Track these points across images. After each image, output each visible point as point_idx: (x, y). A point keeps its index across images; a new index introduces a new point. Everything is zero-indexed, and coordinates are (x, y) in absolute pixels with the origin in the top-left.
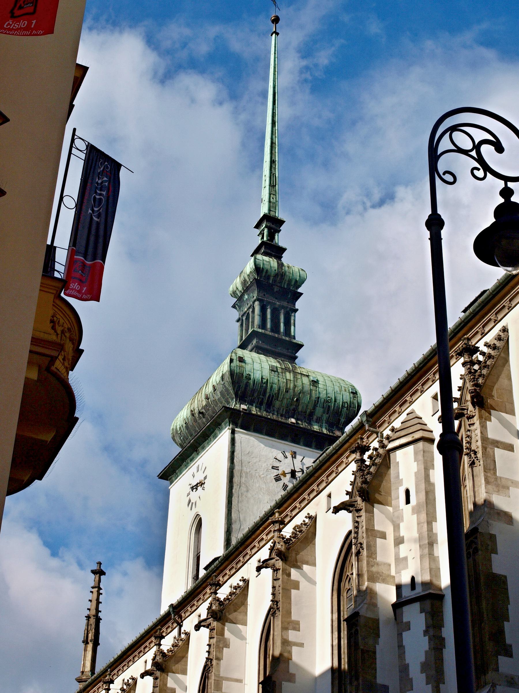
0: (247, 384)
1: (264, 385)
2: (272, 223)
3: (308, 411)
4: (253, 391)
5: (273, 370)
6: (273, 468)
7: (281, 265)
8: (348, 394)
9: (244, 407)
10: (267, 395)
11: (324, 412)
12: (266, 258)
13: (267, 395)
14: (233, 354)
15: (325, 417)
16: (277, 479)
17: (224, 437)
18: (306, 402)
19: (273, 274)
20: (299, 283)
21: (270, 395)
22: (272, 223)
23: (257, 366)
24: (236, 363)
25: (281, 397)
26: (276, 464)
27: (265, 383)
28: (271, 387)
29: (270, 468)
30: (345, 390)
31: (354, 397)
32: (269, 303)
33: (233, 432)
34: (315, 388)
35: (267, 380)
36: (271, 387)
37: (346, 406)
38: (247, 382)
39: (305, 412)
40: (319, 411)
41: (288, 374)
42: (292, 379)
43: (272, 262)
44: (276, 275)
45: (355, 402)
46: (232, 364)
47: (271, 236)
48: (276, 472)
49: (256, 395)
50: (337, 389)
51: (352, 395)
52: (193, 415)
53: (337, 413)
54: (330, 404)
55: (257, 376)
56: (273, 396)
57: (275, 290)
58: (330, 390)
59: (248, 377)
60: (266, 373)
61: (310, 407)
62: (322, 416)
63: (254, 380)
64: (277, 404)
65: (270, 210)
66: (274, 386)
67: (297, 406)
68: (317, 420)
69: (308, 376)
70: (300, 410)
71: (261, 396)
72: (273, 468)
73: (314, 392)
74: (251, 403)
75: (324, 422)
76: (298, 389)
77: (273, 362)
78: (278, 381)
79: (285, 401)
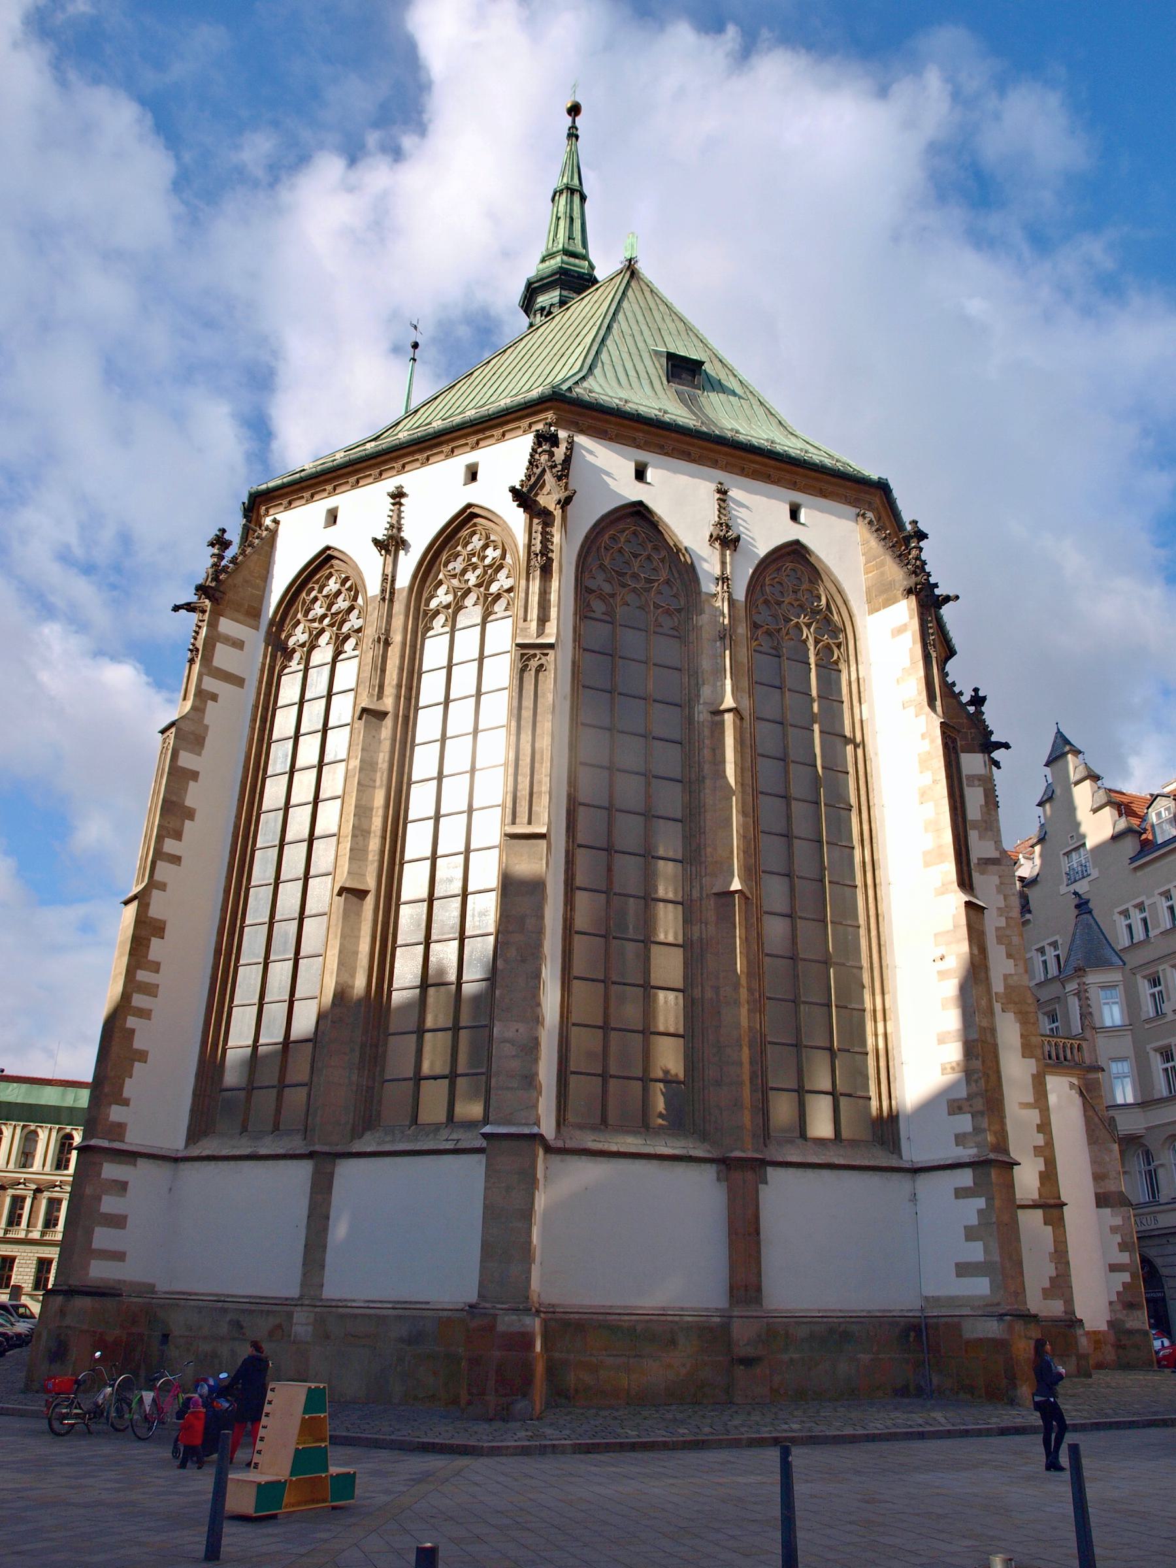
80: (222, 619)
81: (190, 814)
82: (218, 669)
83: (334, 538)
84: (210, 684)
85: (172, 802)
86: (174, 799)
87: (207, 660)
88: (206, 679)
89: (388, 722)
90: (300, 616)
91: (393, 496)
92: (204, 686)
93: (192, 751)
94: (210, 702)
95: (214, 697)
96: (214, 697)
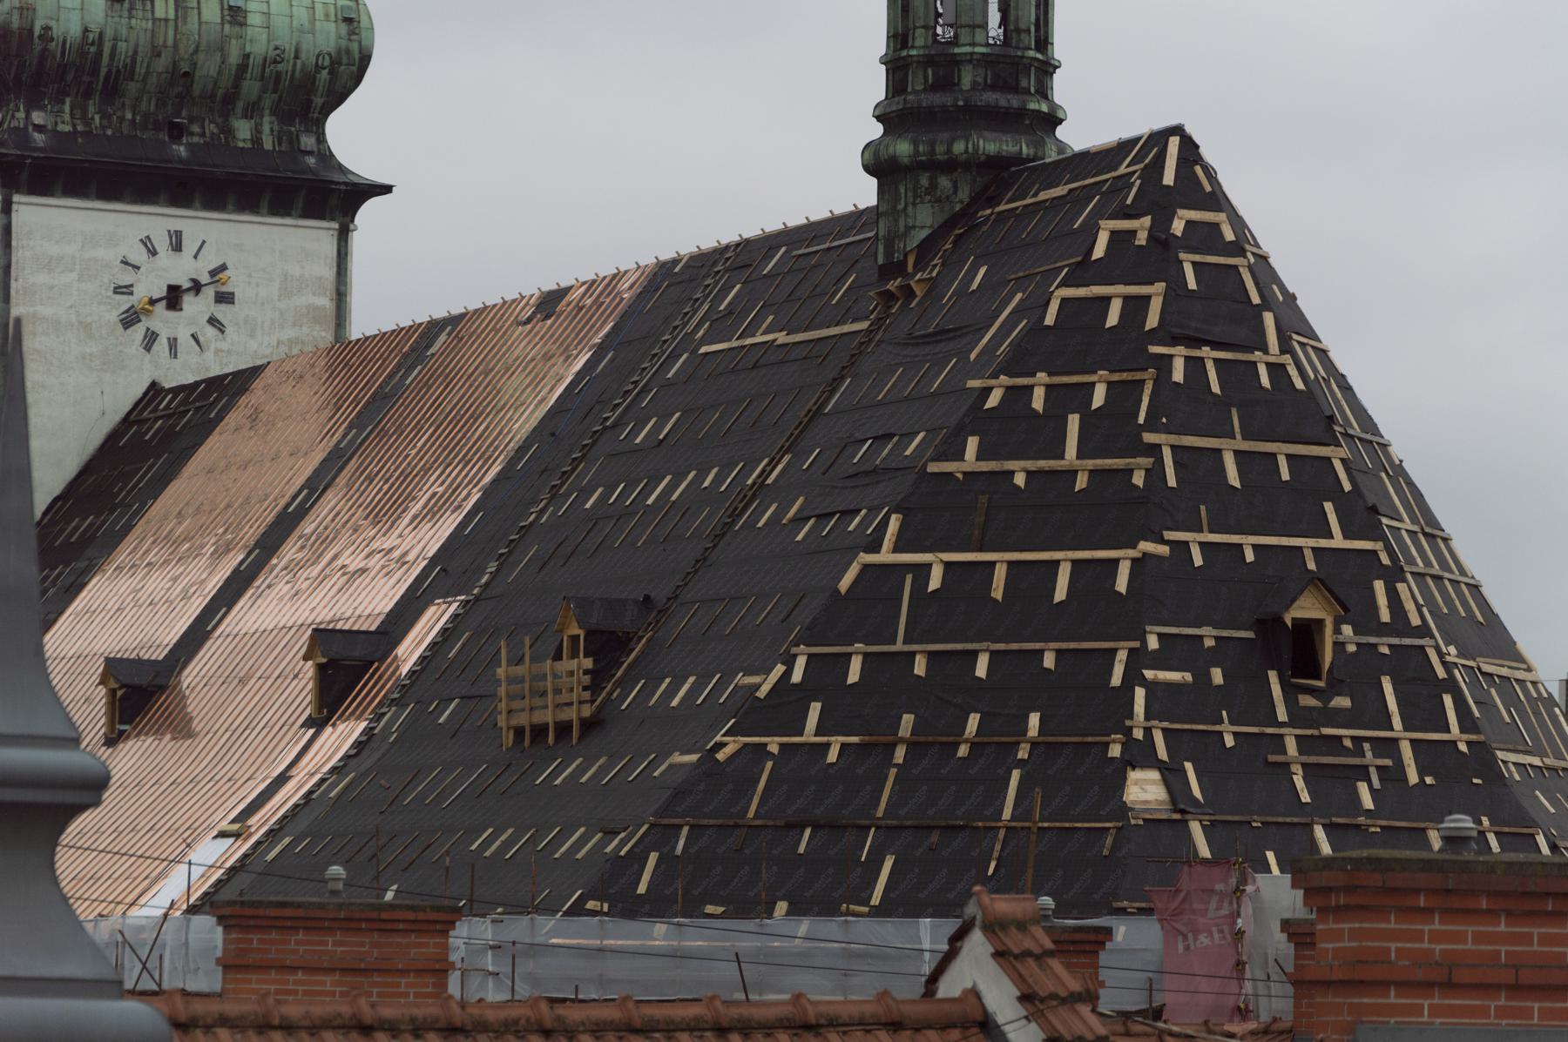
1: (93, 49)
3: (220, 93)
6: (121, 290)
8: (332, 26)
10: (104, 71)
11: (264, 90)
13: (104, 71)
15: (267, 102)
16: (130, 319)
18: (213, 72)
21: (109, 71)
25: (140, 70)
26: (127, 278)
27: (93, 44)
28: (114, 49)
29: (110, 293)
30: (327, 15)
31: (352, 33)
34: (237, 29)
35: (101, 34)
36: (114, 49)
37: (327, 63)
38: (45, 50)
39: (213, 96)
40: (250, 87)
42: (171, 15)
45: (355, 47)
48: (125, 302)
49: (70, 76)
50: (301, 15)
51: (344, 28)
53: (306, 82)
54: (280, 67)
55: (70, 27)
56: (118, 72)
58: (281, 24)
61: (226, 82)
62: (260, 98)
63: (64, 42)
66: (122, 46)
67: (189, 88)
68: (246, 110)
70: (197, 90)
71: (86, 79)
72: (121, 290)
73: (233, 41)
75: (267, 112)
76: (186, 48)
79: (153, 79)
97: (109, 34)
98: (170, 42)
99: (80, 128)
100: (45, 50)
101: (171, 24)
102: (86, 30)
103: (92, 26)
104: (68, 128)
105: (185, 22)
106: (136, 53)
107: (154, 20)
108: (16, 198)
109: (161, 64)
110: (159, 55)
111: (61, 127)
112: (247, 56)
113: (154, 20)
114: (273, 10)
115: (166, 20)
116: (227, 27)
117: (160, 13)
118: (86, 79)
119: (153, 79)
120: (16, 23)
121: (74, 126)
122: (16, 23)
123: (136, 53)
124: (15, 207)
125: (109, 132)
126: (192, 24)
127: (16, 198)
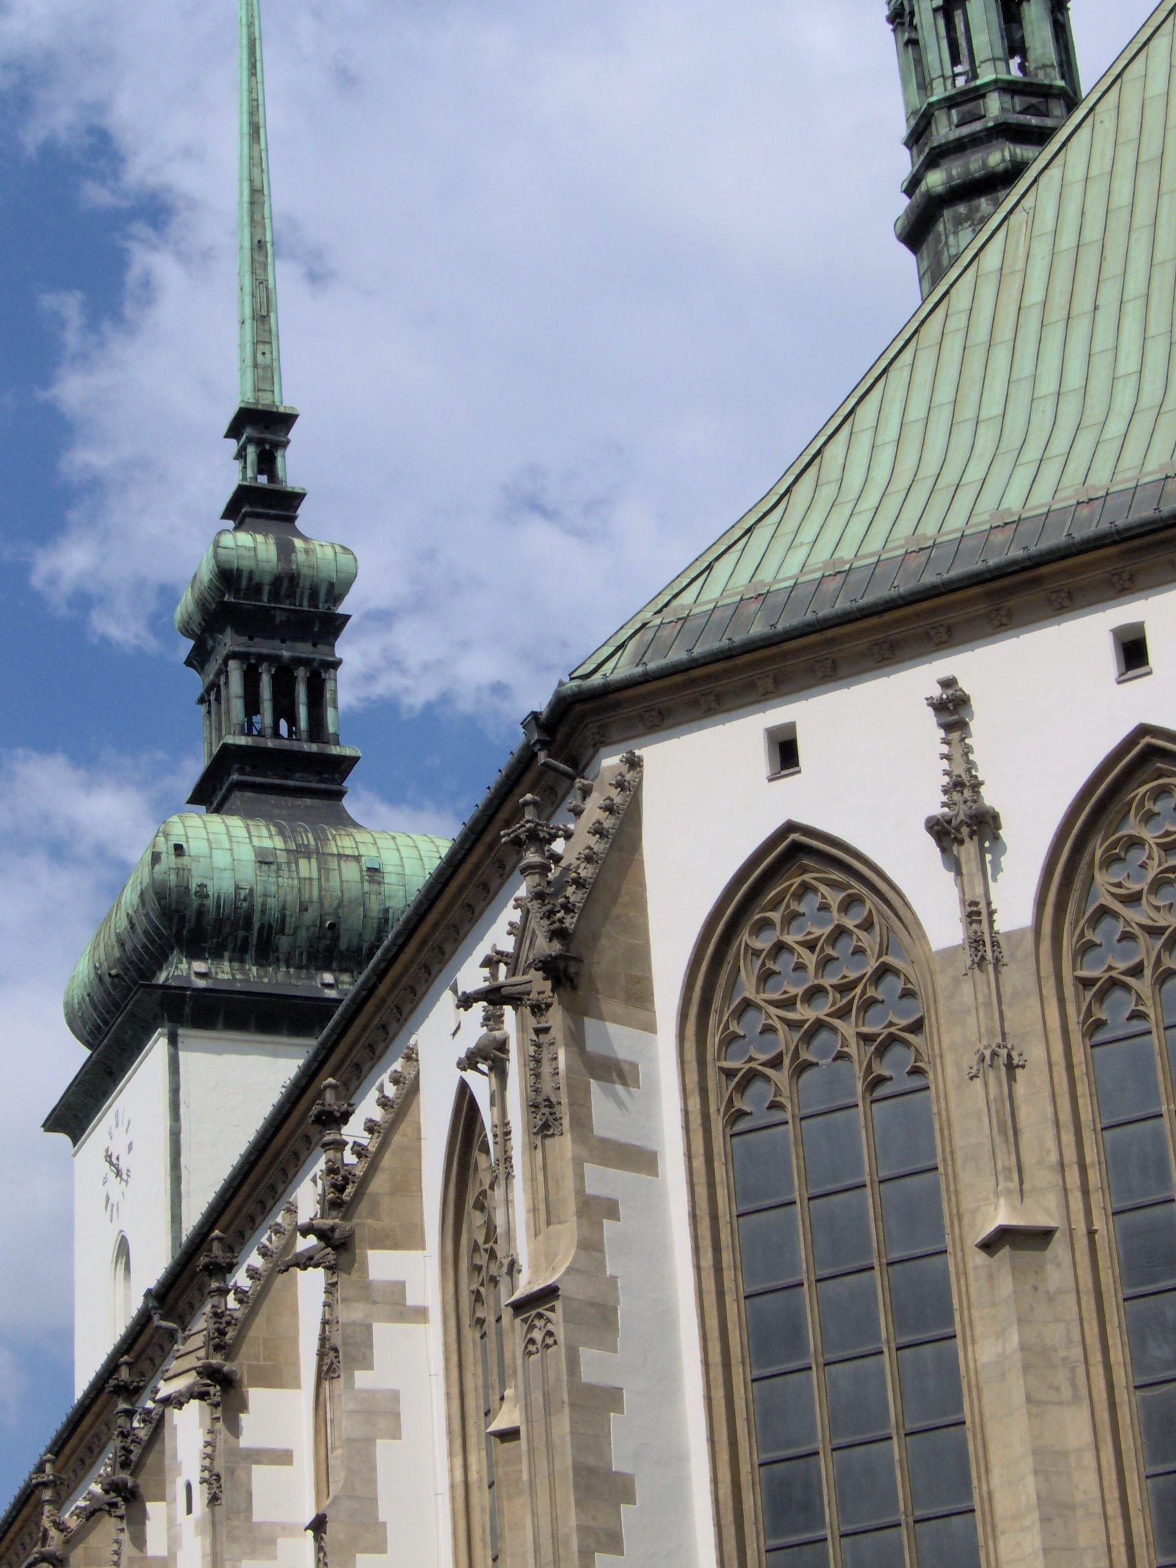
0: (201, 912)
1: (245, 905)
2: (262, 428)
4: (219, 921)
5: (264, 860)
7: (285, 550)
9: (199, 966)
10: (256, 926)
12: (244, 538)
13: (256, 926)
14: (161, 839)
17: (157, 1050)
19: (267, 579)
20: (336, 591)
22: (262, 428)
23: (221, 859)
24: (169, 860)
25: (290, 922)
27: (245, 900)
32: (262, 658)
33: (173, 1041)
34: (376, 886)
35: (251, 890)
36: (264, 905)
38: (202, 905)
39: (360, 949)
41: (303, 863)
42: (315, 875)
43: (261, 549)
44: (277, 581)
46: (157, 867)
47: (267, 462)
49: (226, 930)
52: (100, 978)
57: (278, 620)
59: (202, 893)
60: (248, 874)
61: (369, 936)
63: (219, 897)
64: (284, 942)
65: (257, 389)
67: (336, 939)
69: (357, 858)
70: (343, 945)
71: (241, 933)
73: (373, 897)
74: (217, 955)
77: (267, 838)
78: (278, 889)
79: (303, 934)
80: (587, 1020)
81: (622, 1489)
82: (604, 1141)
83: (808, 801)
84: (603, 1180)
85: (592, 1471)
86: (592, 1460)
87: (582, 1123)
88: (592, 1170)
89: (1058, 1246)
90: (748, 987)
91: (939, 707)
92: (590, 1190)
93: (600, 1345)
94: (607, 1223)
95: (610, 1209)
96: (610, 1209)
97: (259, 889)
98: (315, 893)
99: (238, 977)
100: (202, 905)
101: (315, 883)
102: (237, 888)
103: (243, 885)
104: (226, 977)
105: (328, 880)
106: (284, 908)
107: (299, 879)
108: (181, 1031)
109: (311, 916)
110: (306, 910)
111: (220, 976)
112: (387, 910)
113: (299, 879)
114: (408, 872)
115: (311, 879)
116: (366, 885)
117: (304, 872)
118: (241, 933)
119: (303, 934)
120: (173, 879)
121: (233, 975)
122: (173, 879)
123: (284, 908)
124: (180, 1039)
125: (266, 980)
126: (335, 883)
127: (181, 1031)
